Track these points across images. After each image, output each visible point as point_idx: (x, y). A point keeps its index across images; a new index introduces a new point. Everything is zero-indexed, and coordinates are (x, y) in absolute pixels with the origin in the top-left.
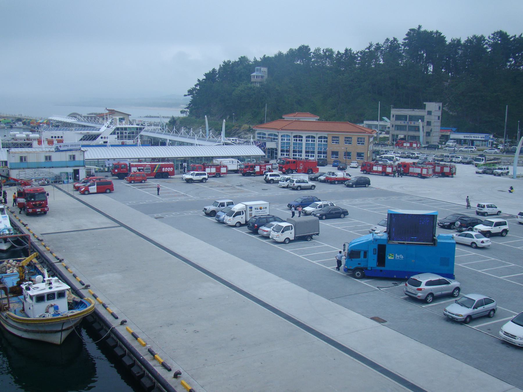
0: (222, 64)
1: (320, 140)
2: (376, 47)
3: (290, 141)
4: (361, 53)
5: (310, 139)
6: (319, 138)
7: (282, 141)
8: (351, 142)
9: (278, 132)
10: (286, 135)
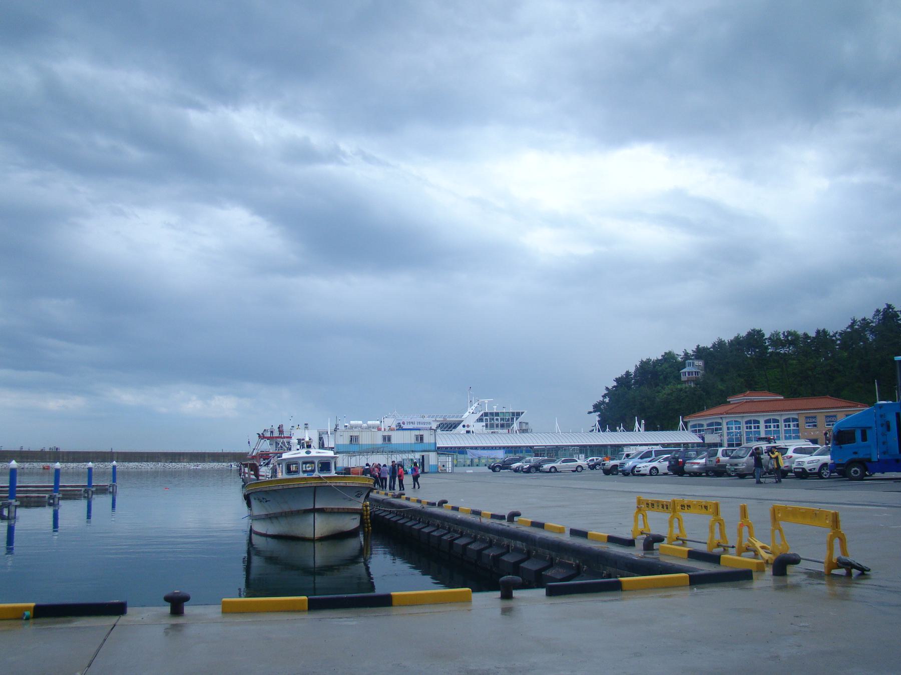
0: (638, 364)
2: (863, 323)
3: (741, 430)
4: (841, 334)
5: (772, 425)
6: (785, 421)
9: (721, 418)
10: (735, 421)
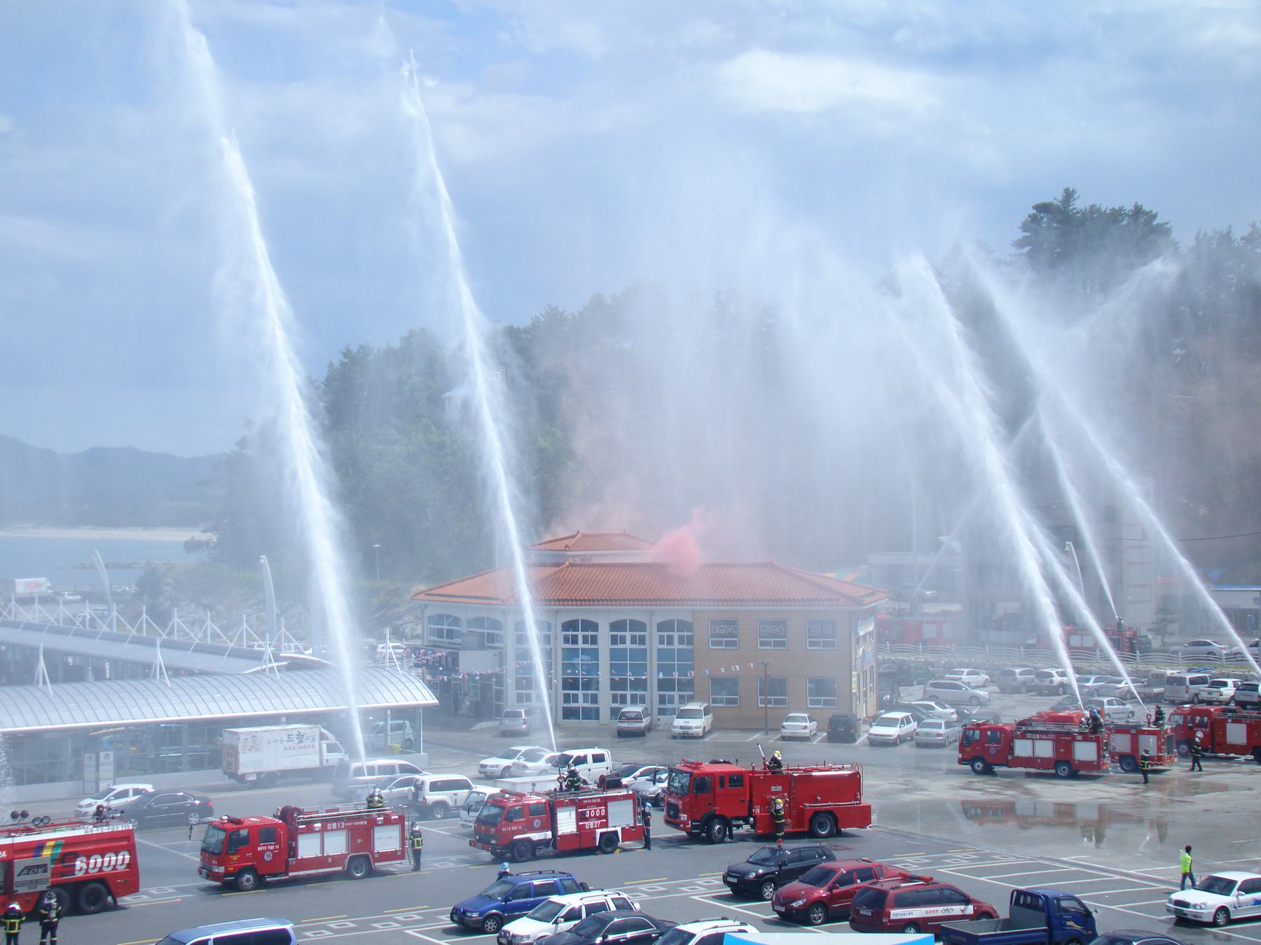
1: (666, 634)
5: (628, 635)
6: (662, 627)
7: (519, 646)
8: (783, 636)
